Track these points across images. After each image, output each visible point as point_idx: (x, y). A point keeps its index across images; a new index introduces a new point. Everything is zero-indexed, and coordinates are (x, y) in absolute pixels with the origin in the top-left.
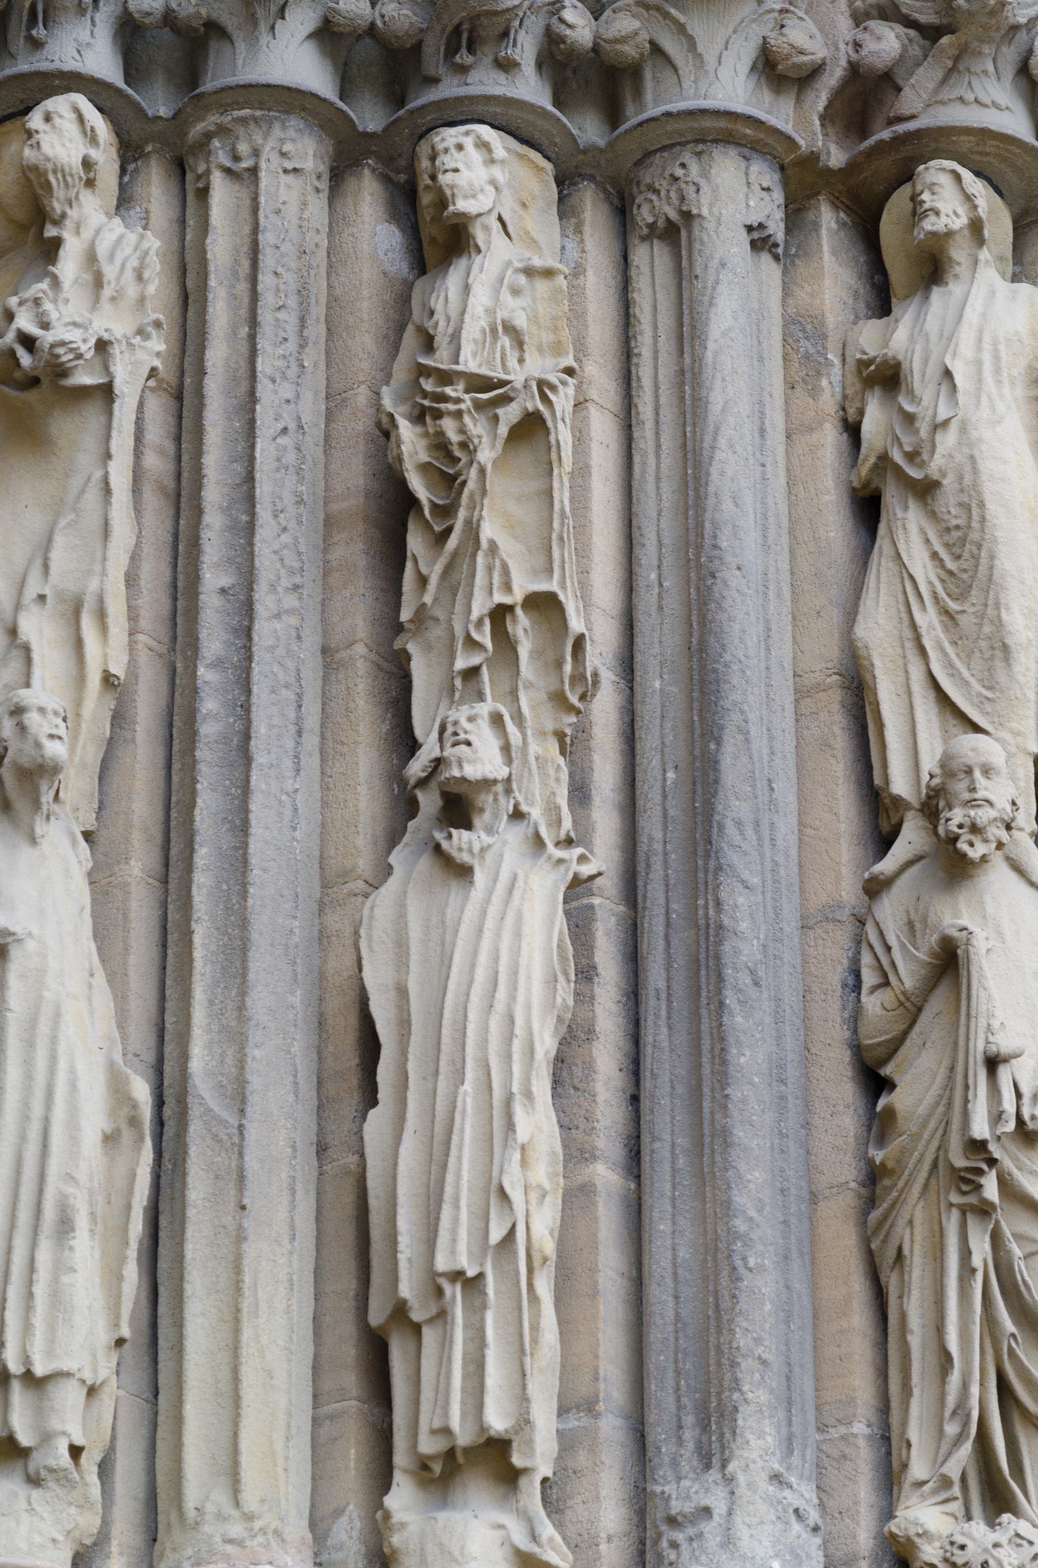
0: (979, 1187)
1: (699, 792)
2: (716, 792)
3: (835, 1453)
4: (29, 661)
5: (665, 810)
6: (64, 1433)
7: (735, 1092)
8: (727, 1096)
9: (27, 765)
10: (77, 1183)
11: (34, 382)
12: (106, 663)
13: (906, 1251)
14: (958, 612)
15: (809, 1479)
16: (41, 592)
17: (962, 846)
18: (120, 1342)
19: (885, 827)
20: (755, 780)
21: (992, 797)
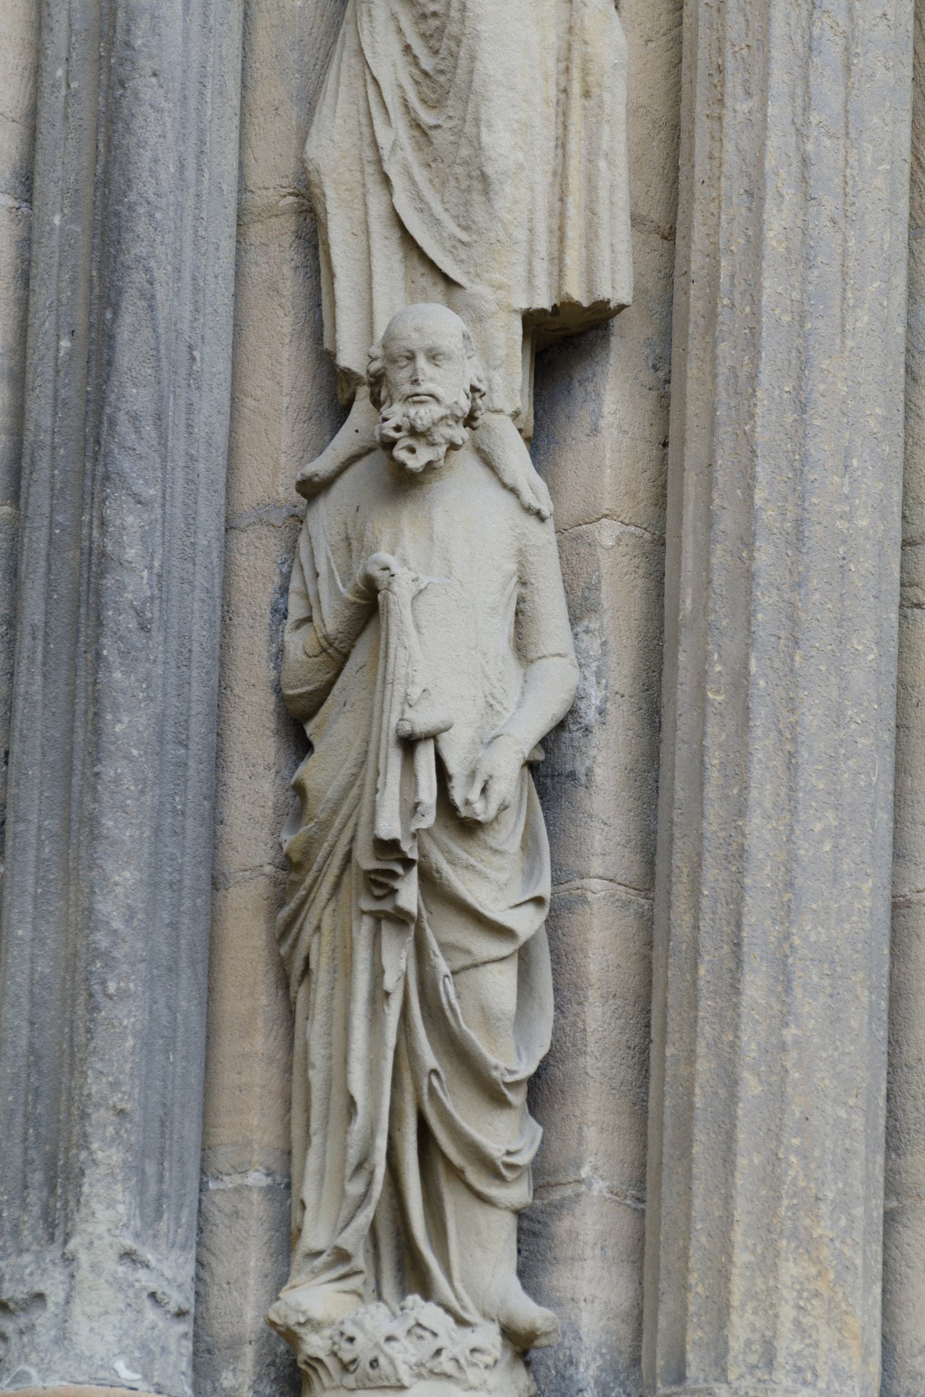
0: (394, 892)
1: (93, 372)
2: (108, 376)
3: (228, 1208)
5: (56, 390)
7: (108, 771)
8: (97, 774)
13: (313, 965)
14: (431, 128)
15: (183, 1248)
17: (400, 454)
19: (343, 397)
20: (159, 360)
21: (439, 391)
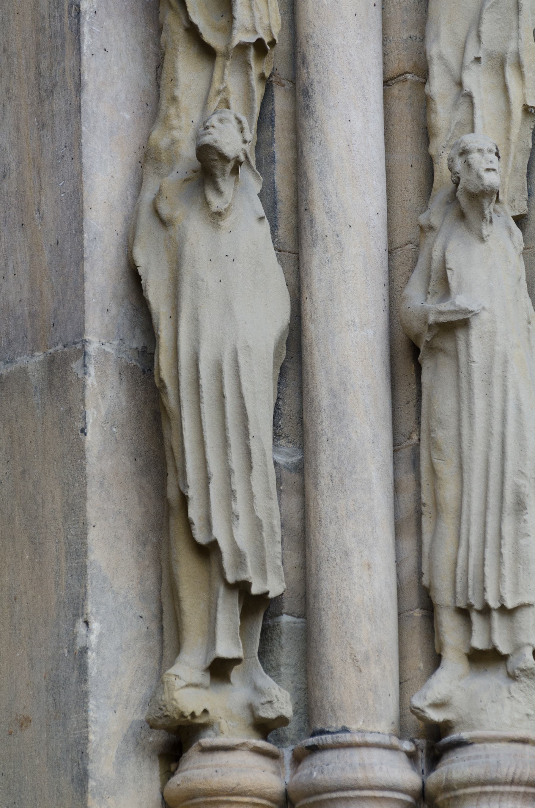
4: (472, 104)
6: (529, 644)
9: (473, 190)
10: (526, 476)
12: (524, 100)
16: (476, 56)
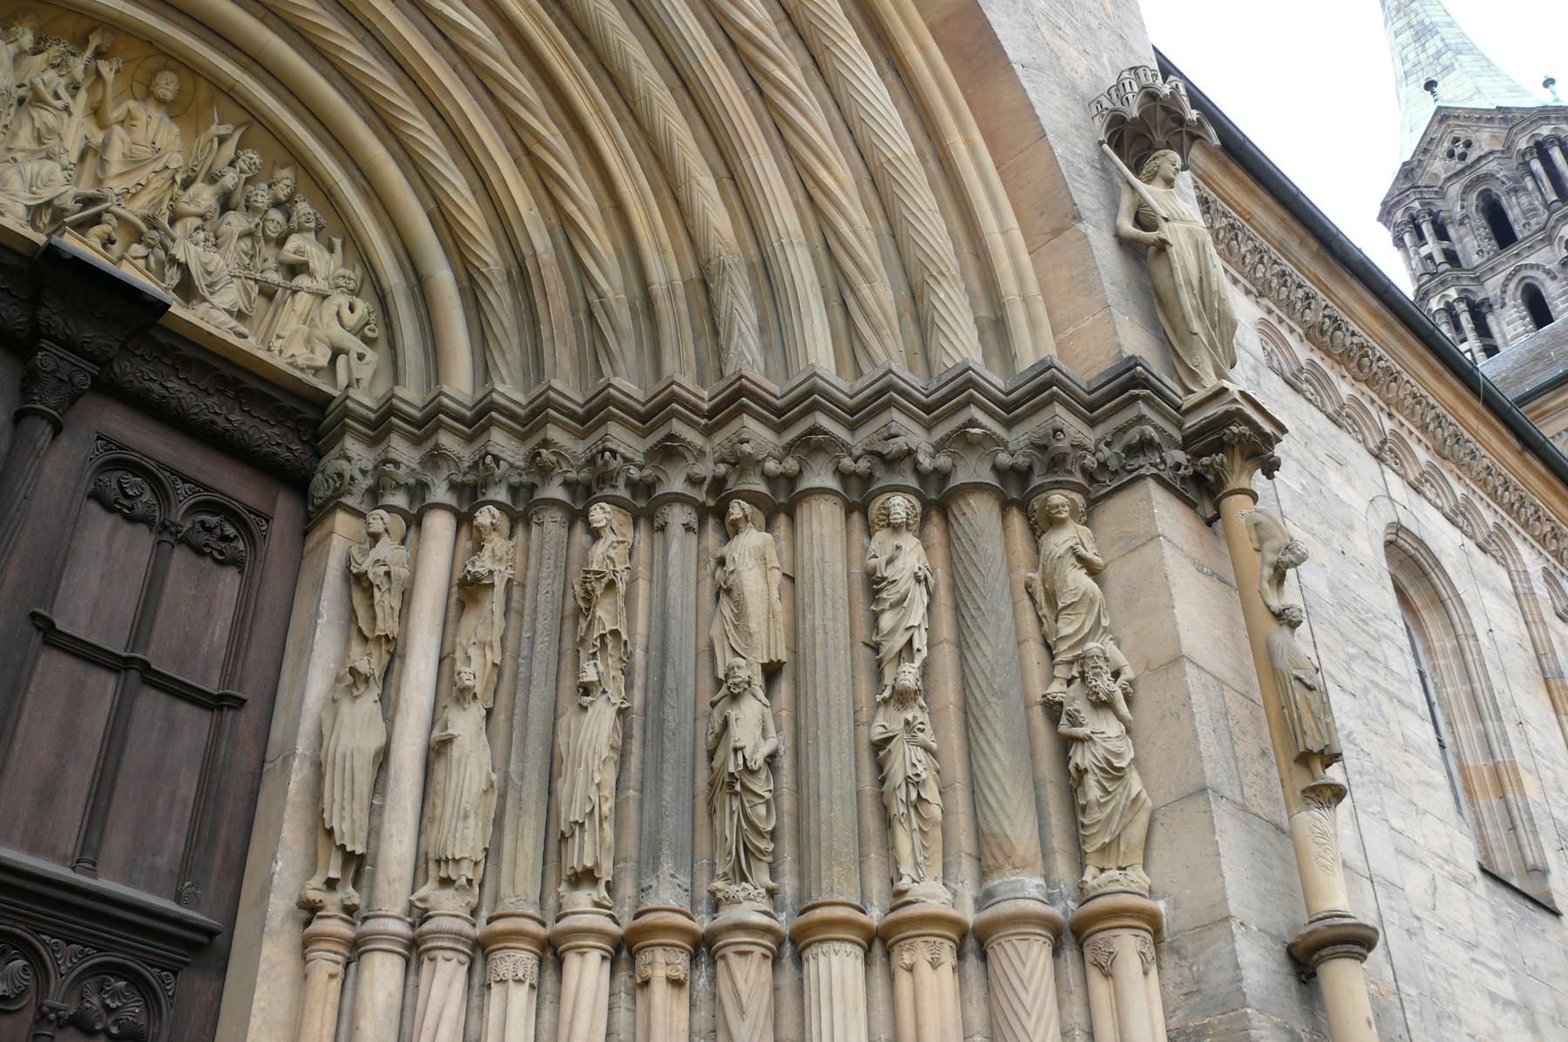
11: (472, 584)
18: (485, 849)
